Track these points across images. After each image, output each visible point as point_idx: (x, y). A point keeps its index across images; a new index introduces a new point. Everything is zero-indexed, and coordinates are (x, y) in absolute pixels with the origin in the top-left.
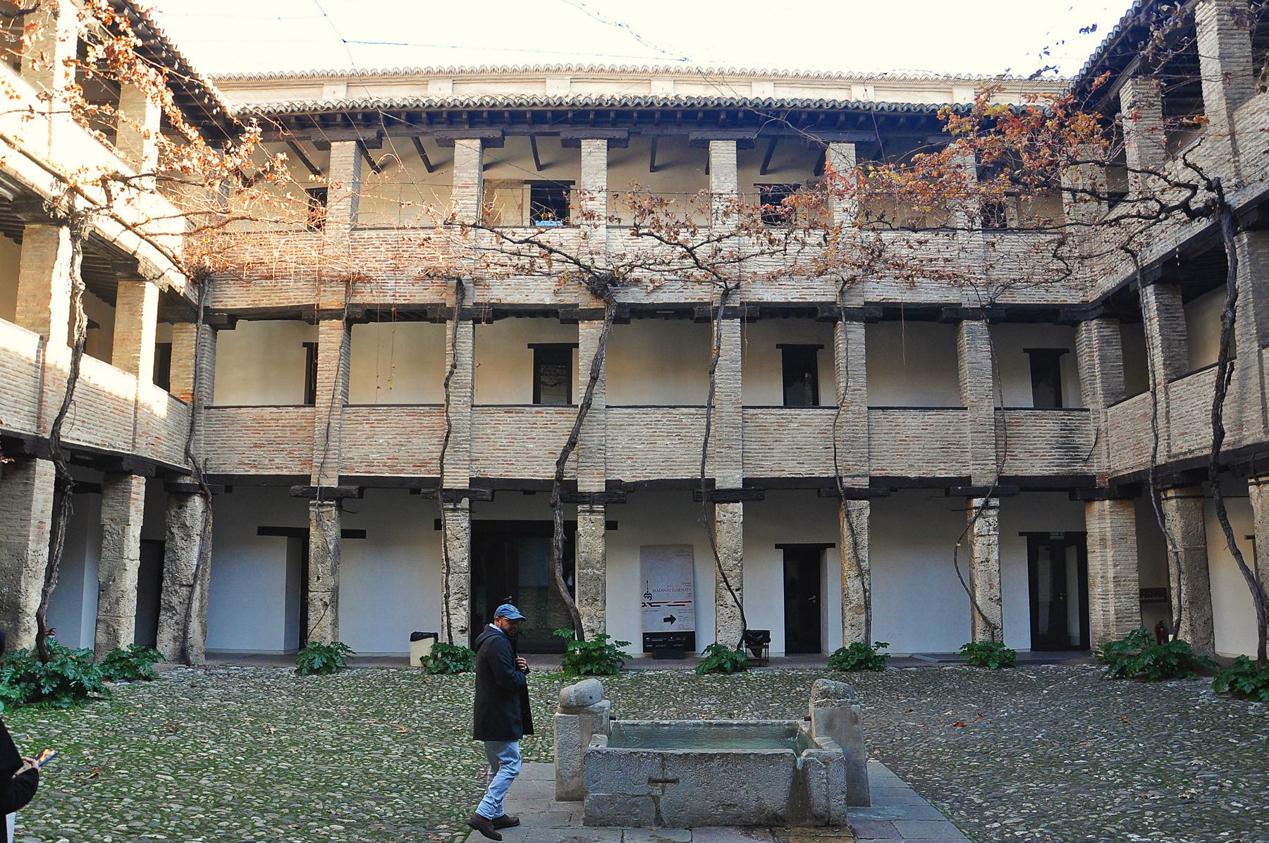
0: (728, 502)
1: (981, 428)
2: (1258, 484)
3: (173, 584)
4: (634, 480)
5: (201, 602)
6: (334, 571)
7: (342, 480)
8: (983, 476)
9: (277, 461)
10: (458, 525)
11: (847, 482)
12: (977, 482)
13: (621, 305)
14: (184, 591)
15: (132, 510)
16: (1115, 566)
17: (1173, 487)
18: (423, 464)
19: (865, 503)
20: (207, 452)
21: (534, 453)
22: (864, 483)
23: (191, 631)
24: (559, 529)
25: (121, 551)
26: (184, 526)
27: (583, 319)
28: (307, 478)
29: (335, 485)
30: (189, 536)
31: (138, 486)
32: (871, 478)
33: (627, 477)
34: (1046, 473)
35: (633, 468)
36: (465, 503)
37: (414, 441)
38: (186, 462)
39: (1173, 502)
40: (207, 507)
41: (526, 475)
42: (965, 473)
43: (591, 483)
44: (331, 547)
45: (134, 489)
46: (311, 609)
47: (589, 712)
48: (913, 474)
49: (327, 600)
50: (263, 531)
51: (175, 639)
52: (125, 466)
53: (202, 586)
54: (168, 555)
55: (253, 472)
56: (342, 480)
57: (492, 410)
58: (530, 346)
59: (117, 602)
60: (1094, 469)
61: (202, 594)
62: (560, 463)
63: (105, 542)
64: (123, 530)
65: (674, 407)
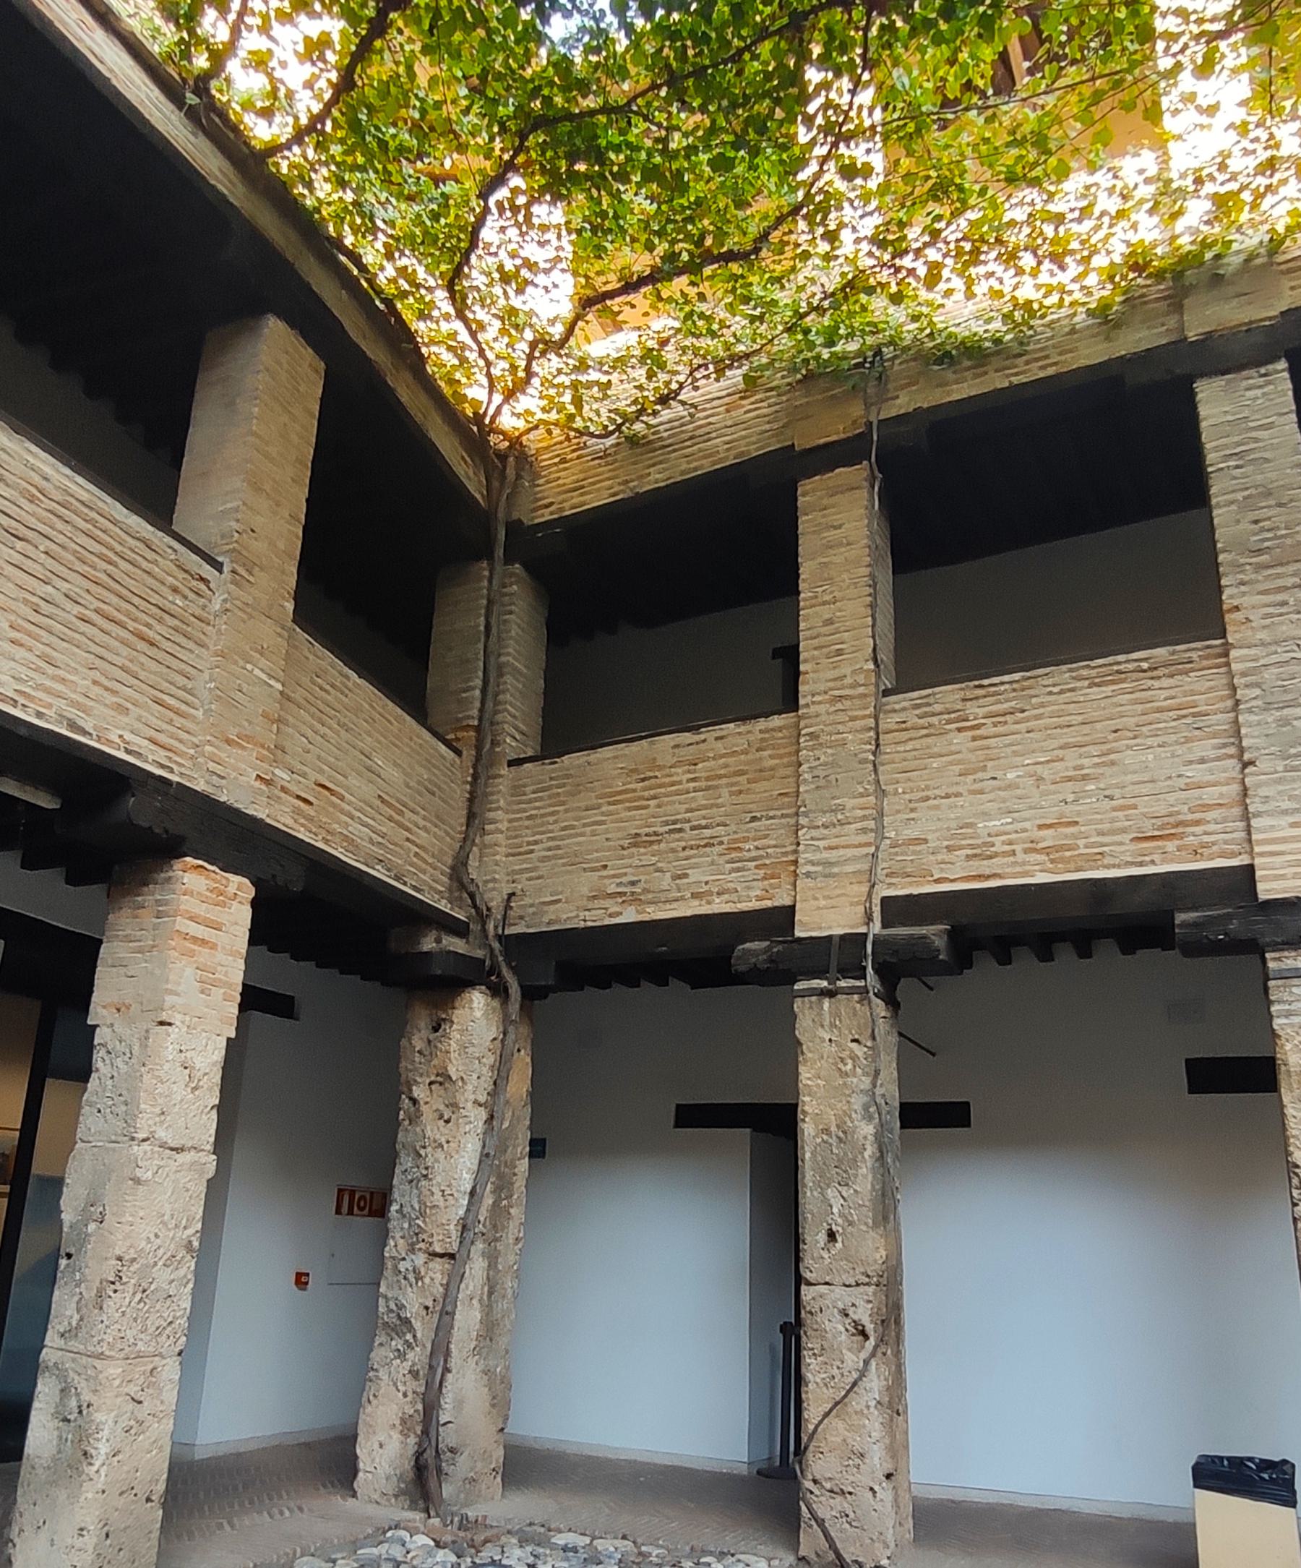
5: (488, 1308)
6: (885, 1210)
9: (694, 875)
14: (437, 1273)
18: (1170, 830)
20: (513, 878)
23: (448, 1401)
25: (130, 1119)
26: (443, 1079)
30: (454, 1106)
37: (1128, 758)
40: (506, 1021)
45: (188, 904)
46: (810, 1343)
50: (690, 1116)
53: (492, 1259)
54: (406, 1161)
55: (630, 915)
56: (896, 910)
61: (492, 1287)
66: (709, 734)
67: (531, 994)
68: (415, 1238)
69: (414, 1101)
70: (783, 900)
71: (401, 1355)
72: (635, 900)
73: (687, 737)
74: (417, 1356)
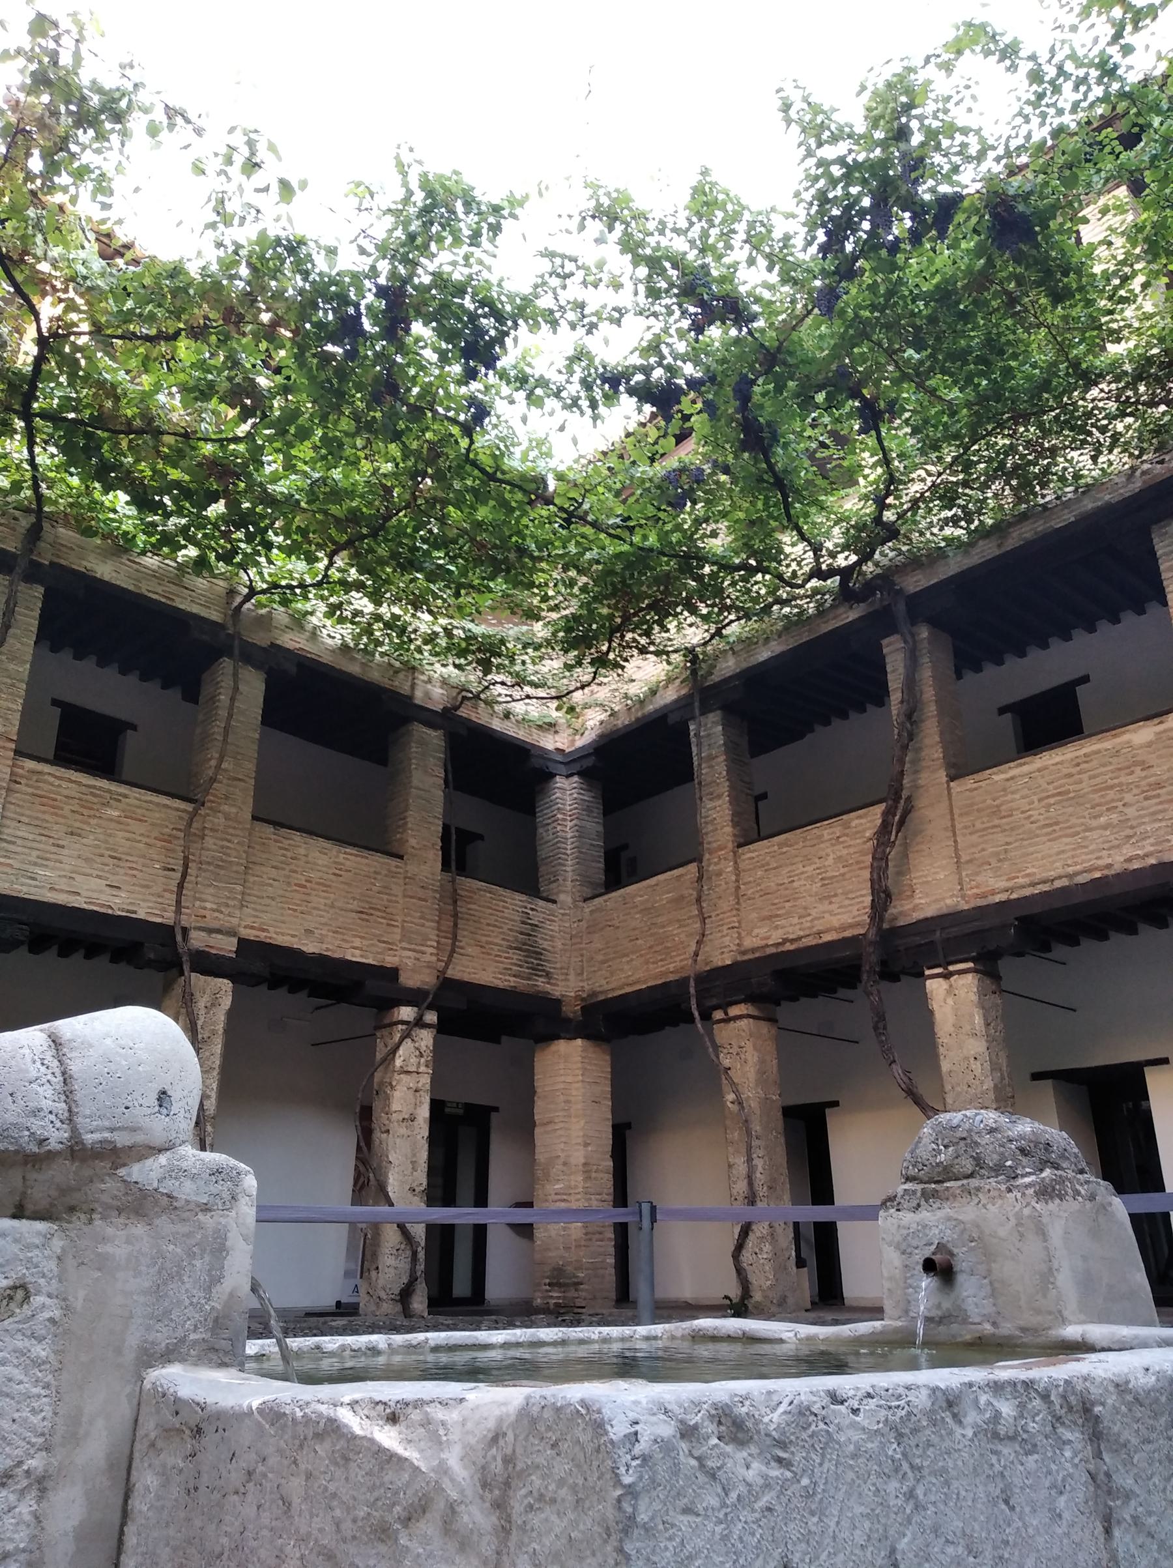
1: (421, 893)
2: (947, 976)
8: (417, 974)
11: (198, 940)
12: (410, 980)
16: (586, 1145)
17: (750, 999)
19: (225, 985)
22: (226, 946)
32: (242, 942)
34: (501, 985)
39: (743, 1023)
42: (390, 961)
47: (141, 1204)
48: (310, 947)
60: (557, 991)
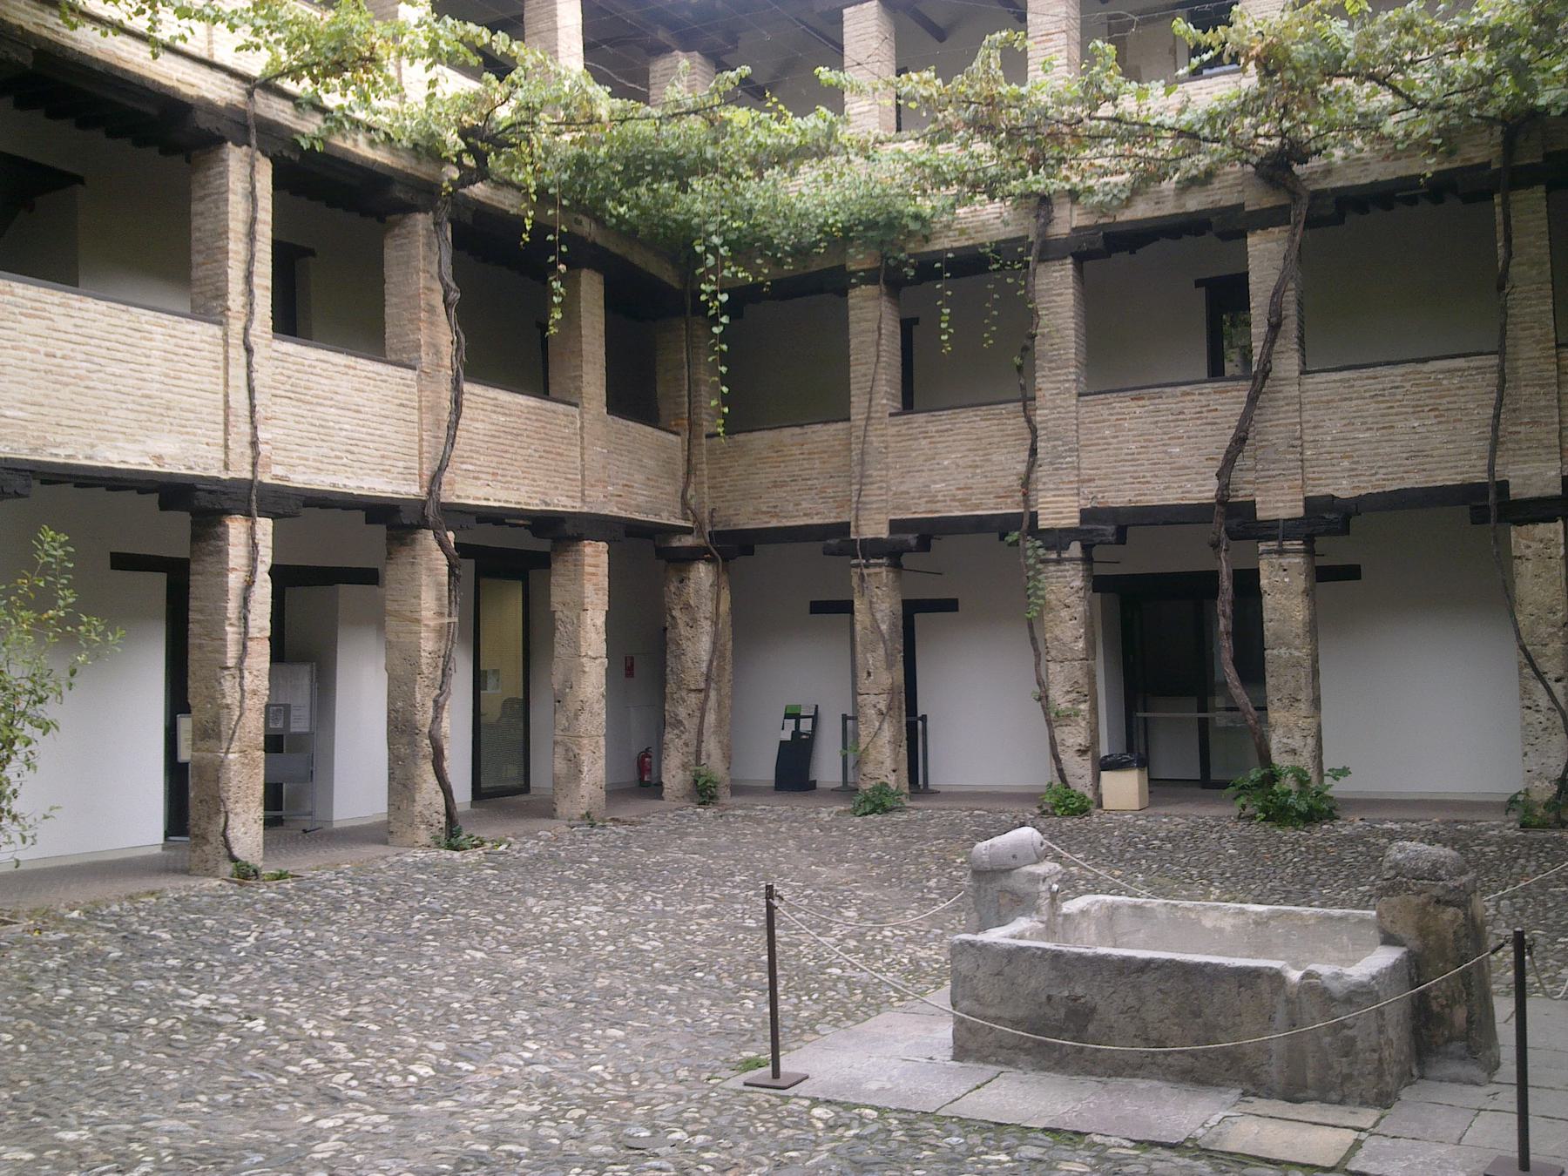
0: (1535, 521)
3: (679, 688)
4: (1356, 493)
7: (895, 526)
9: (805, 505)
10: (1065, 588)
13: (1317, 195)
14: (693, 699)
15: (589, 589)
21: (1183, 462)
24: (1226, 583)
25: (578, 647)
26: (687, 607)
27: (1254, 229)
28: (843, 529)
29: (885, 536)
30: (695, 620)
31: (595, 557)
33: (1344, 489)
35: (1352, 473)
36: (1075, 549)
38: (687, 519)
40: (718, 576)
41: (1171, 497)
43: (1279, 502)
44: (884, 627)
45: (588, 560)
49: (882, 706)
51: (685, 766)
52: (569, 529)
53: (719, 690)
55: (774, 523)
56: (895, 526)
57: (1111, 397)
58: (1198, 283)
59: (576, 717)
62: (1224, 473)
63: (558, 635)
64: (578, 617)
65: (1425, 361)
66: (809, 429)
67: (725, 560)
68: (680, 684)
69: (673, 618)
70: (845, 519)
71: (679, 737)
72: (776, 515)
73: (797, 430)
74: (690, 736)
